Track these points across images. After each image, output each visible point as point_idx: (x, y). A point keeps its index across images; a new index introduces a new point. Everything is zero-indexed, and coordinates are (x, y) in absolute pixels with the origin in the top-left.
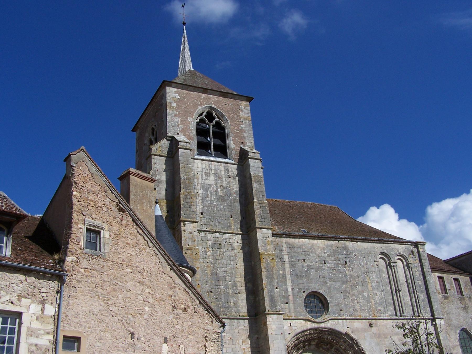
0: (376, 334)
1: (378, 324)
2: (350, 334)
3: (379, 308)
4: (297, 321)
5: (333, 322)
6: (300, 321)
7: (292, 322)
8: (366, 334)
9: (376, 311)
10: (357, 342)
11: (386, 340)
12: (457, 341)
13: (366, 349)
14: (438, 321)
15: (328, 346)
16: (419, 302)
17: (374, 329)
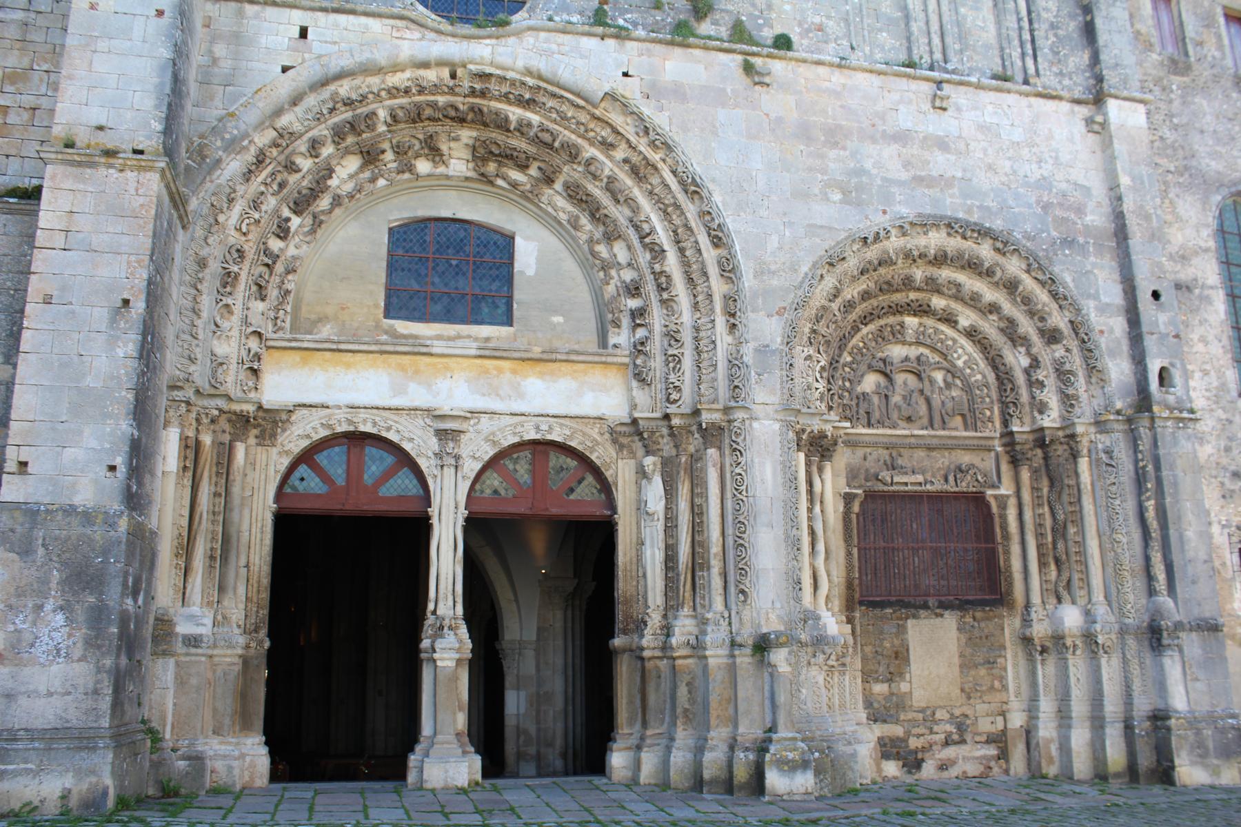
0: (779, 120)
1: (803, 81)
2: (631, 101)
3: (817, 20)
4: (342, 19)
5: (547, 41)
6: (363, 20)
7: (316, 20)
8: (722, 114)
9: (800, 24)
10: (665, 143)
11: (832, 154)
12: (1205, 233)
13: (713, 181)
14: (1120, 107)
15: (533, 171)
16: (1032, 31)
17: (772, 102)
